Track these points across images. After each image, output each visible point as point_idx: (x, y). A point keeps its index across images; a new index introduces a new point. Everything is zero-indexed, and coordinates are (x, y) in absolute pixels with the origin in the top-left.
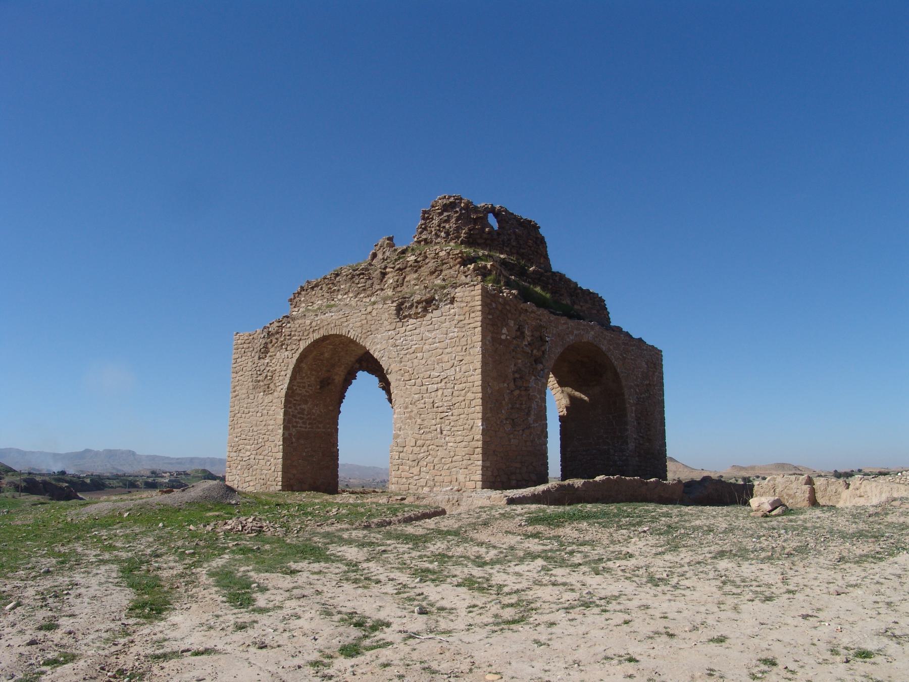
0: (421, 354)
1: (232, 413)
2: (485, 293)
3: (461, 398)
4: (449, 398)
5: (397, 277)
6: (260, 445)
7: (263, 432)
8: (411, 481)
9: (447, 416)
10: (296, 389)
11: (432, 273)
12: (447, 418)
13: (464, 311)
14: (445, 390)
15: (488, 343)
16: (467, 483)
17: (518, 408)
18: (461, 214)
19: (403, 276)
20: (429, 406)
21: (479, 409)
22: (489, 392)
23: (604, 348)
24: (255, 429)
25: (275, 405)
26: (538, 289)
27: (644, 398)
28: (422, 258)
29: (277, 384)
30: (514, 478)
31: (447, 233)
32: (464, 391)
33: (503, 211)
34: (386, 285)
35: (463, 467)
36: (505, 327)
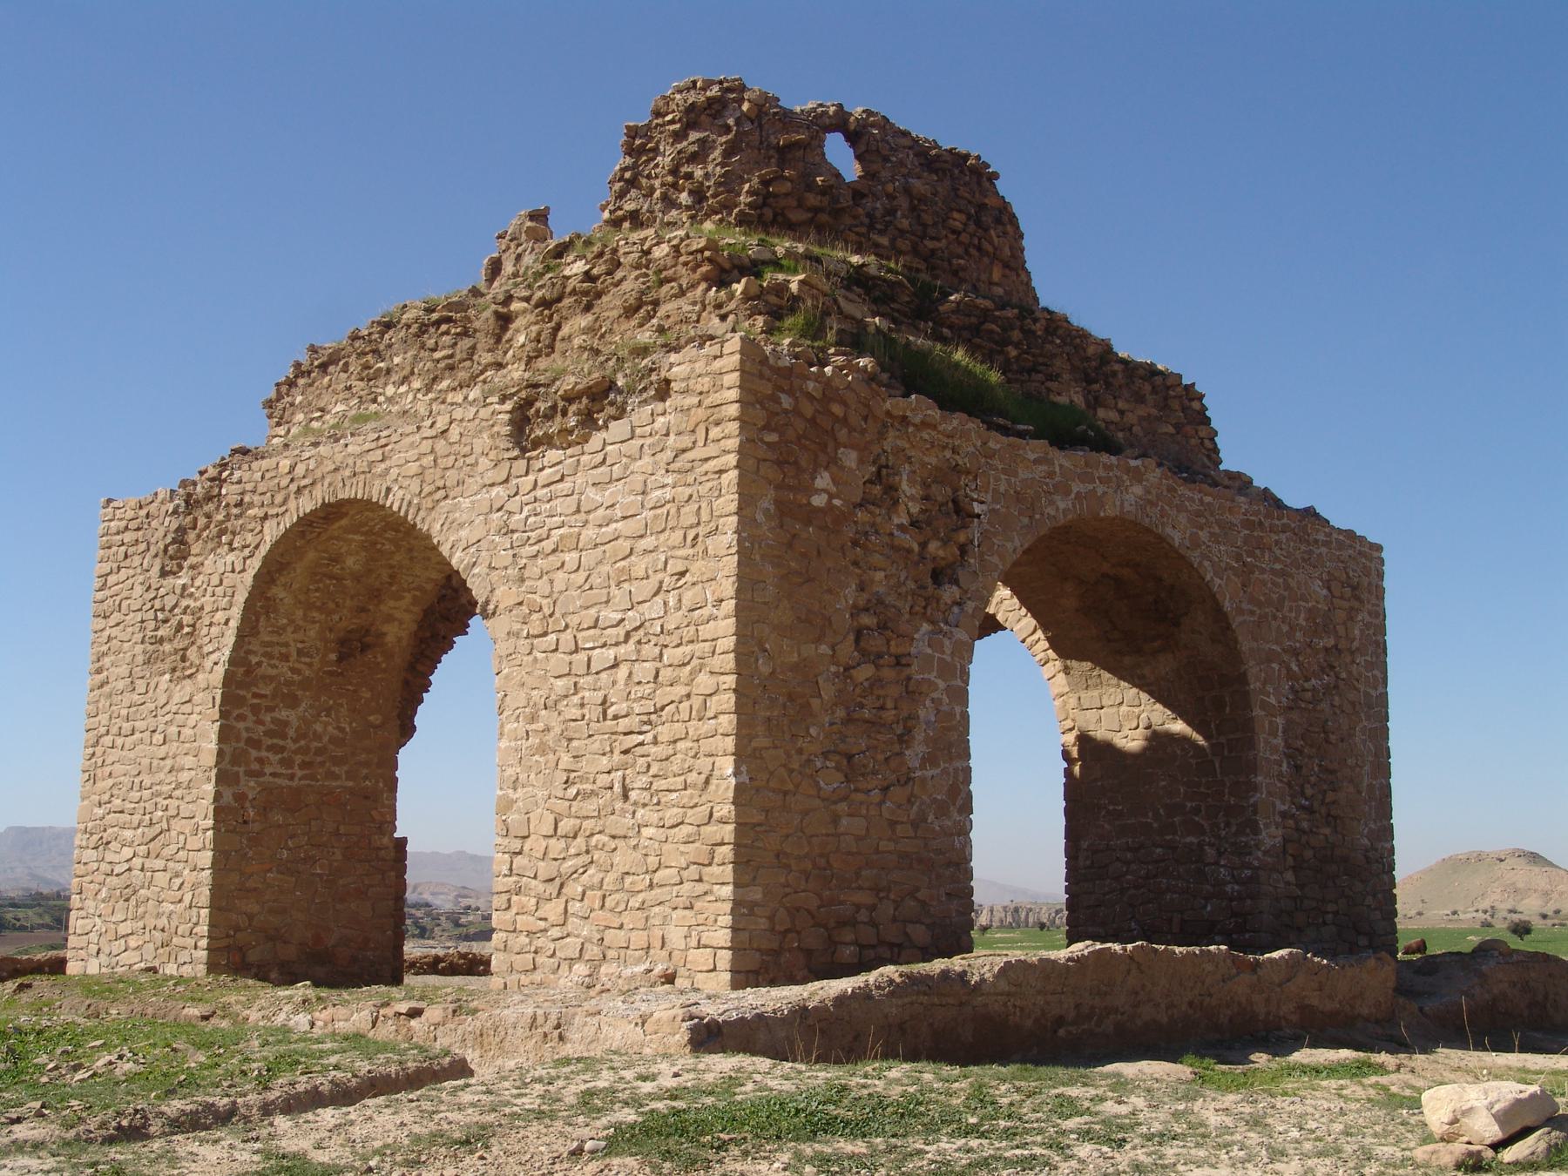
0: (575, 555)
1: (91, 734)
2: (754, 365)
3: (681, 690)
4: (648, 689)
5: (535, 328)
6: (157, 828)
7: (166, 789)
8: (539, 943)
9: (641, 744)
10: (259, 664)
11: (630, 311)
12: (639, 750)
14: (637, 665)
15: (760, 517)
17: (867, 722)
19: (553, 324)
20: (593, 712)
21: (728, 722)
22: (765, 669)
23: (1176, 537)
24: (147, 783)
25: (197, 709)
26: (959, 355)
27: (1314, 689)
28: (603, 267)
29: (206, 649)
30: (849, 937)
31: (699, 195)
32: (688, 668)
33: (873, 125)
34: (511, 352)
35: (681, 902)
36: (826, 468)
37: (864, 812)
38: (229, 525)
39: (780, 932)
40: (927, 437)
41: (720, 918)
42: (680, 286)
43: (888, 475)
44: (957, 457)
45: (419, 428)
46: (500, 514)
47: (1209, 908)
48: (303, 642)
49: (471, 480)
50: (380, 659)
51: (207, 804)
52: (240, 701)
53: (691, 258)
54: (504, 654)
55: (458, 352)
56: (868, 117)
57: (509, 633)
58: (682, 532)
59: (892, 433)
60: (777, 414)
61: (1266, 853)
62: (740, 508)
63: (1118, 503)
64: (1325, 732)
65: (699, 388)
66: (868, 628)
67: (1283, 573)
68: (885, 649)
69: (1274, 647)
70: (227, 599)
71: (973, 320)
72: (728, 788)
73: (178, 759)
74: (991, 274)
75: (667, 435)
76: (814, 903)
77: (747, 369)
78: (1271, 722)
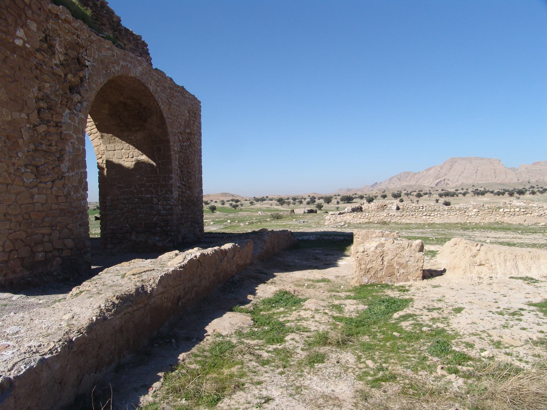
17: (44, 151)
23: (151, 88)
27: (186, 146)
37: (45, 192)
39: (8, 252)
40: (66, 26)
43: (50, 40)
44: (79, 40)
47: (155, 219)
63: (135, 72)
66: (43, 108)
67: (178, 106)
68: (51, 119)
69: (176, 131)
78: (175, 156)
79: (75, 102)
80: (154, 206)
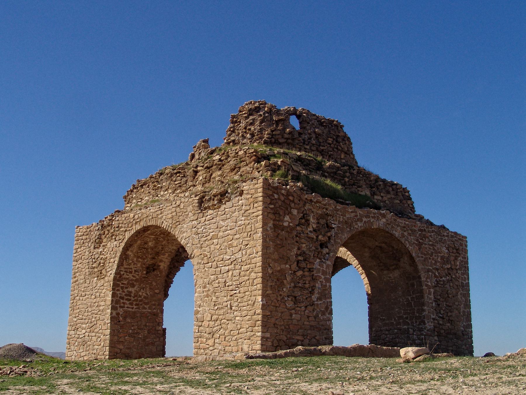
0: (217, 240)
1: (72, 296)
2: (267, 186)
3: (247, 278)
5: (205, 175)
6: (93, 324)
9: (236, 293)
10: (123, 274)
11: (232, 170)
13: (250, 202)
14: (234, 271)
15: (269, 229)
16: (250, 352)
17: (300, 287)
18: (265, 117)
19: (210, 174)
20: (222, 285)
21: (259, 286)
22: (270, 271)
24: (90, 310)
25: (105, 288)
26: (328, 182)
27: (443, 281)
28: (225, 157)
29: (108, 270)
31: (253, 135)
32: (249, 271)
34: (198, 182)
36: (288, 215)
37: (300, 313)
38: (115, 233)
39: (275, 346)
40: (318, 205)
41: (258, 342)
42: (247, 163)
43: (306, 216)
45: (171, 204)
46: (195, 229)
48: (136, 268)
49: (187, 219)
50: (158, 273)
51: (108, 316)
52: (118, 285)
53: (249, 155)
54: (196, 269)
55: (182, 182)
56: (303, 111)
57: (198, 263)
58: (247, 233)
59: (307, 204)
60: (273, 200)
61: (428, 330)
62: (263, 226)
63: (378, 224)
64: (447, 294)
65: (251, 193)
66: (301, 260)
67: (432, 245)
68: (306, 267)
69: (430, 268)
70: (114, 255)
71: (334, 170)
72: (260, 305)
73: (99, 303)
74: (341, 156)
75: (242, 206)
76: (285, 338)
77: (265, 187)
78: (429, 291)
79: (324, 254)
80: (410, 336)
